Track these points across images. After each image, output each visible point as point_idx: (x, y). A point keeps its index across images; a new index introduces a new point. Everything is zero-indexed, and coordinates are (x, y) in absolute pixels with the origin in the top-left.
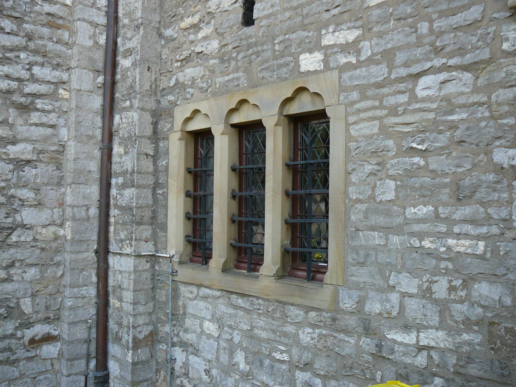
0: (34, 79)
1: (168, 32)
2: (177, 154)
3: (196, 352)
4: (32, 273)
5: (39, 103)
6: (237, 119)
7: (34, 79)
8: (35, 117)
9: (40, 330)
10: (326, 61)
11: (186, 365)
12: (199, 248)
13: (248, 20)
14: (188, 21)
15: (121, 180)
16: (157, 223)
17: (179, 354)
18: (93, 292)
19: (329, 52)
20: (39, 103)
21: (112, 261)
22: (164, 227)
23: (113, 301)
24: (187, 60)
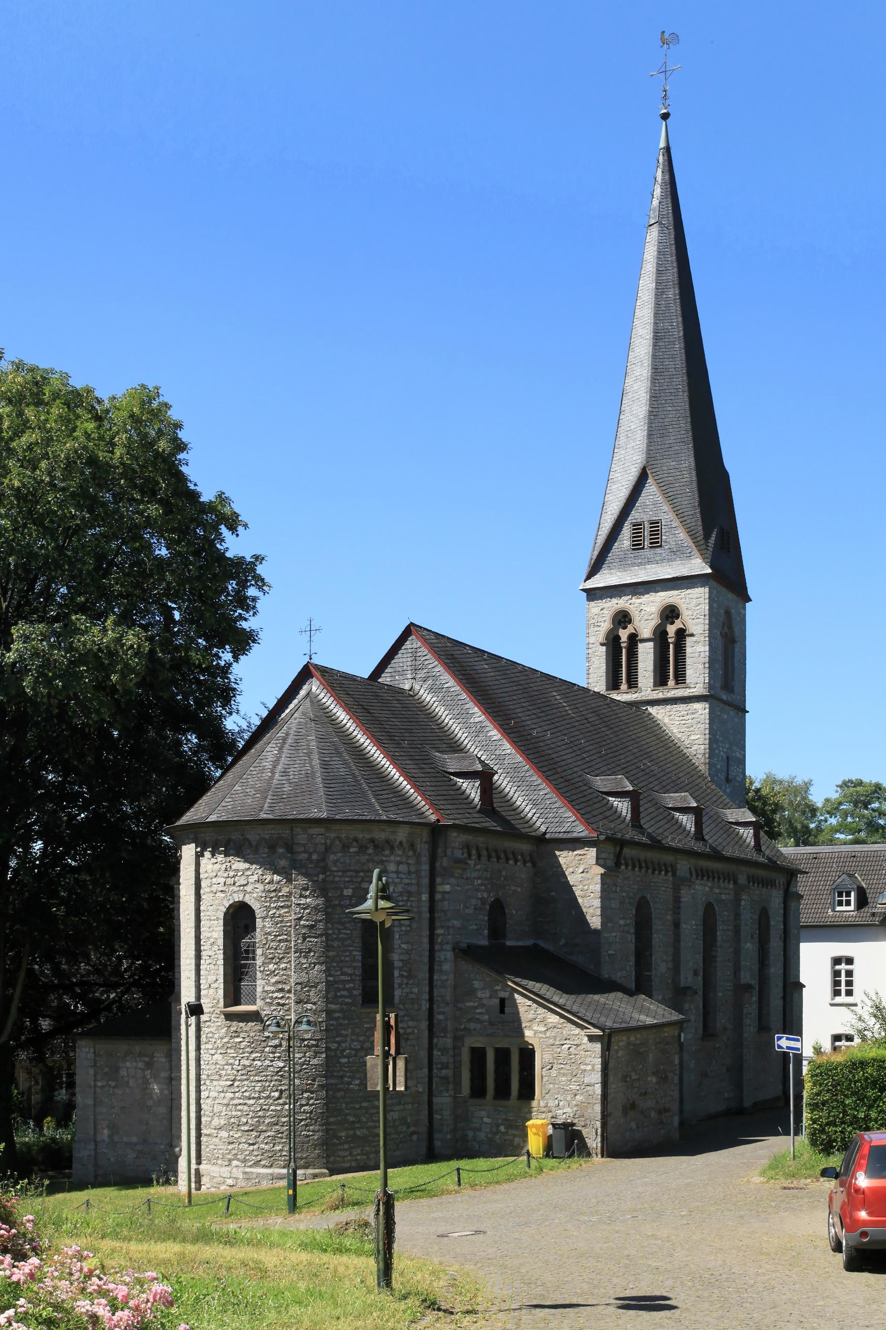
0: (409, 1027)
1: (459, 1005)
2: (465, 1056)
3: (480, 1130)
4: (410, 1106)
5: (411, 1037)
6: (497, 1046)
7: (409, 1027)
8: (409, 1043)
9: (412, 1129)
10: (535, 1034)
11: (474, 1137)
12: (478, 1091)
13: (502, 1011)
14: (472, 1004)
15: (440, 1066)
16: (458, 1084)
17: (470, 1134)
18: (427, 1113)
19: (536, 1032)
20: (411, 1037)
21: (434, 1100)
22: (460, 1084)
23: (437, 1116)
24: (470, 1020)
